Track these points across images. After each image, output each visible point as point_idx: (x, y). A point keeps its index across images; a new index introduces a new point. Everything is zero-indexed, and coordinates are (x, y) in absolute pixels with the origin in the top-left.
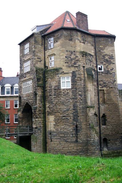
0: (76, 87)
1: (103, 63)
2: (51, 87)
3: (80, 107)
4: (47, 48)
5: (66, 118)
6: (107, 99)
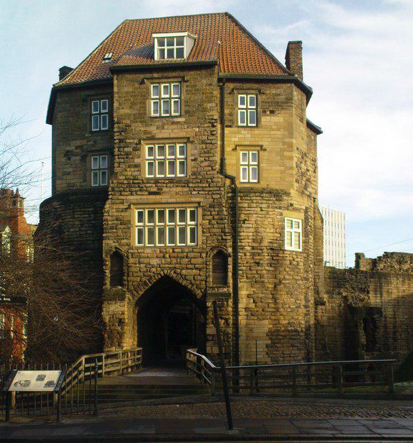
2: (258, 240)
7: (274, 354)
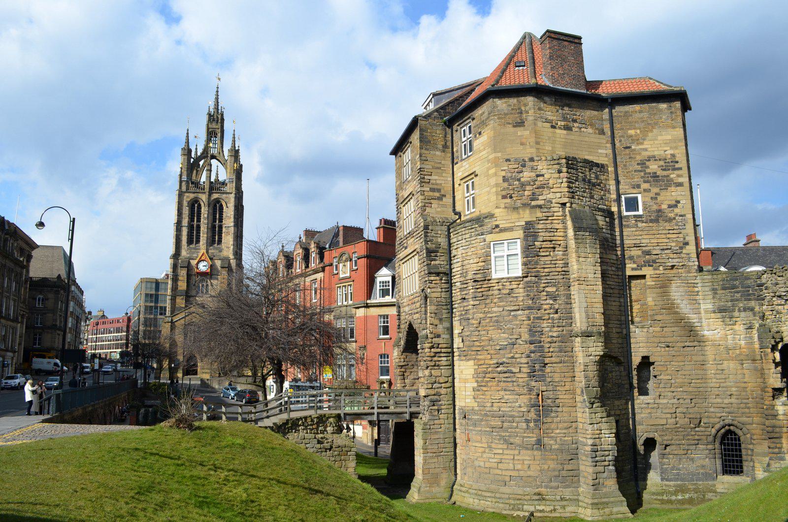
0: (538, 272)
1: (638, 186)
2: (464, 274)
3: (550, 334)
4: (458, 157)
5: (505, 369)
6: (655, 308)
7: (480, 398)
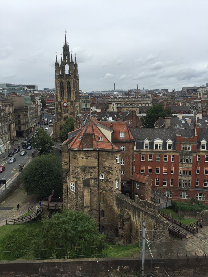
1: (103, 173)
